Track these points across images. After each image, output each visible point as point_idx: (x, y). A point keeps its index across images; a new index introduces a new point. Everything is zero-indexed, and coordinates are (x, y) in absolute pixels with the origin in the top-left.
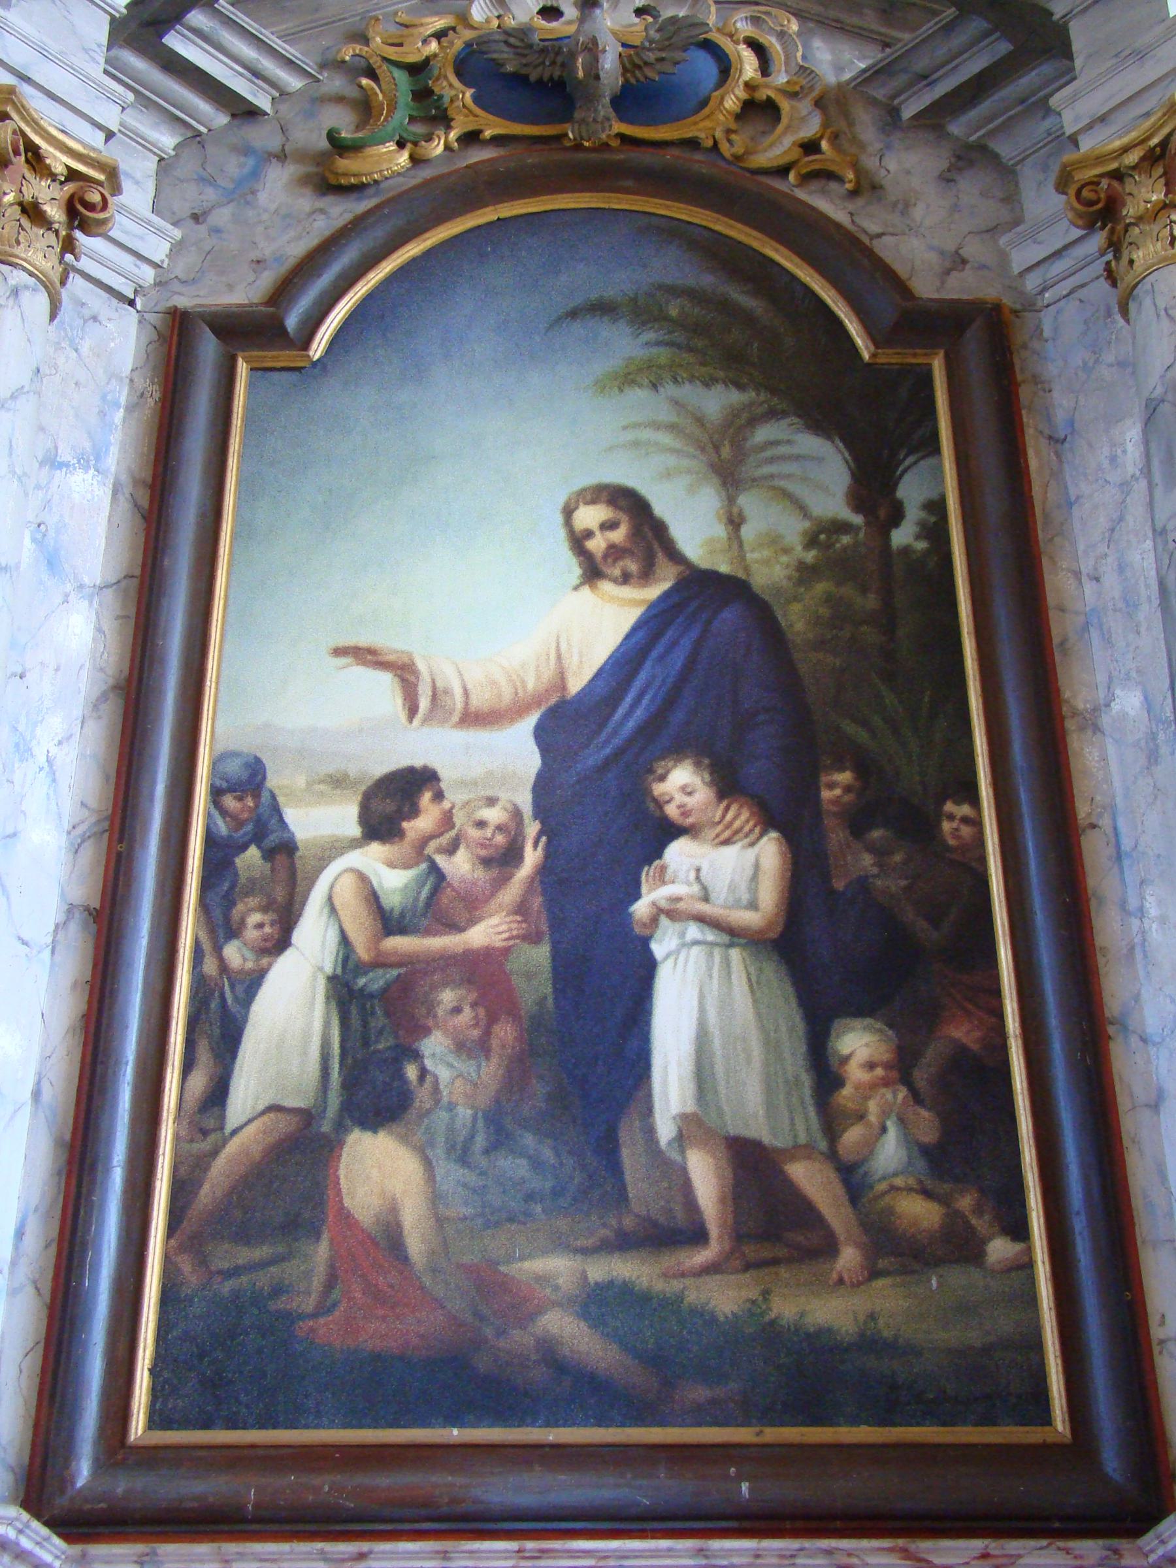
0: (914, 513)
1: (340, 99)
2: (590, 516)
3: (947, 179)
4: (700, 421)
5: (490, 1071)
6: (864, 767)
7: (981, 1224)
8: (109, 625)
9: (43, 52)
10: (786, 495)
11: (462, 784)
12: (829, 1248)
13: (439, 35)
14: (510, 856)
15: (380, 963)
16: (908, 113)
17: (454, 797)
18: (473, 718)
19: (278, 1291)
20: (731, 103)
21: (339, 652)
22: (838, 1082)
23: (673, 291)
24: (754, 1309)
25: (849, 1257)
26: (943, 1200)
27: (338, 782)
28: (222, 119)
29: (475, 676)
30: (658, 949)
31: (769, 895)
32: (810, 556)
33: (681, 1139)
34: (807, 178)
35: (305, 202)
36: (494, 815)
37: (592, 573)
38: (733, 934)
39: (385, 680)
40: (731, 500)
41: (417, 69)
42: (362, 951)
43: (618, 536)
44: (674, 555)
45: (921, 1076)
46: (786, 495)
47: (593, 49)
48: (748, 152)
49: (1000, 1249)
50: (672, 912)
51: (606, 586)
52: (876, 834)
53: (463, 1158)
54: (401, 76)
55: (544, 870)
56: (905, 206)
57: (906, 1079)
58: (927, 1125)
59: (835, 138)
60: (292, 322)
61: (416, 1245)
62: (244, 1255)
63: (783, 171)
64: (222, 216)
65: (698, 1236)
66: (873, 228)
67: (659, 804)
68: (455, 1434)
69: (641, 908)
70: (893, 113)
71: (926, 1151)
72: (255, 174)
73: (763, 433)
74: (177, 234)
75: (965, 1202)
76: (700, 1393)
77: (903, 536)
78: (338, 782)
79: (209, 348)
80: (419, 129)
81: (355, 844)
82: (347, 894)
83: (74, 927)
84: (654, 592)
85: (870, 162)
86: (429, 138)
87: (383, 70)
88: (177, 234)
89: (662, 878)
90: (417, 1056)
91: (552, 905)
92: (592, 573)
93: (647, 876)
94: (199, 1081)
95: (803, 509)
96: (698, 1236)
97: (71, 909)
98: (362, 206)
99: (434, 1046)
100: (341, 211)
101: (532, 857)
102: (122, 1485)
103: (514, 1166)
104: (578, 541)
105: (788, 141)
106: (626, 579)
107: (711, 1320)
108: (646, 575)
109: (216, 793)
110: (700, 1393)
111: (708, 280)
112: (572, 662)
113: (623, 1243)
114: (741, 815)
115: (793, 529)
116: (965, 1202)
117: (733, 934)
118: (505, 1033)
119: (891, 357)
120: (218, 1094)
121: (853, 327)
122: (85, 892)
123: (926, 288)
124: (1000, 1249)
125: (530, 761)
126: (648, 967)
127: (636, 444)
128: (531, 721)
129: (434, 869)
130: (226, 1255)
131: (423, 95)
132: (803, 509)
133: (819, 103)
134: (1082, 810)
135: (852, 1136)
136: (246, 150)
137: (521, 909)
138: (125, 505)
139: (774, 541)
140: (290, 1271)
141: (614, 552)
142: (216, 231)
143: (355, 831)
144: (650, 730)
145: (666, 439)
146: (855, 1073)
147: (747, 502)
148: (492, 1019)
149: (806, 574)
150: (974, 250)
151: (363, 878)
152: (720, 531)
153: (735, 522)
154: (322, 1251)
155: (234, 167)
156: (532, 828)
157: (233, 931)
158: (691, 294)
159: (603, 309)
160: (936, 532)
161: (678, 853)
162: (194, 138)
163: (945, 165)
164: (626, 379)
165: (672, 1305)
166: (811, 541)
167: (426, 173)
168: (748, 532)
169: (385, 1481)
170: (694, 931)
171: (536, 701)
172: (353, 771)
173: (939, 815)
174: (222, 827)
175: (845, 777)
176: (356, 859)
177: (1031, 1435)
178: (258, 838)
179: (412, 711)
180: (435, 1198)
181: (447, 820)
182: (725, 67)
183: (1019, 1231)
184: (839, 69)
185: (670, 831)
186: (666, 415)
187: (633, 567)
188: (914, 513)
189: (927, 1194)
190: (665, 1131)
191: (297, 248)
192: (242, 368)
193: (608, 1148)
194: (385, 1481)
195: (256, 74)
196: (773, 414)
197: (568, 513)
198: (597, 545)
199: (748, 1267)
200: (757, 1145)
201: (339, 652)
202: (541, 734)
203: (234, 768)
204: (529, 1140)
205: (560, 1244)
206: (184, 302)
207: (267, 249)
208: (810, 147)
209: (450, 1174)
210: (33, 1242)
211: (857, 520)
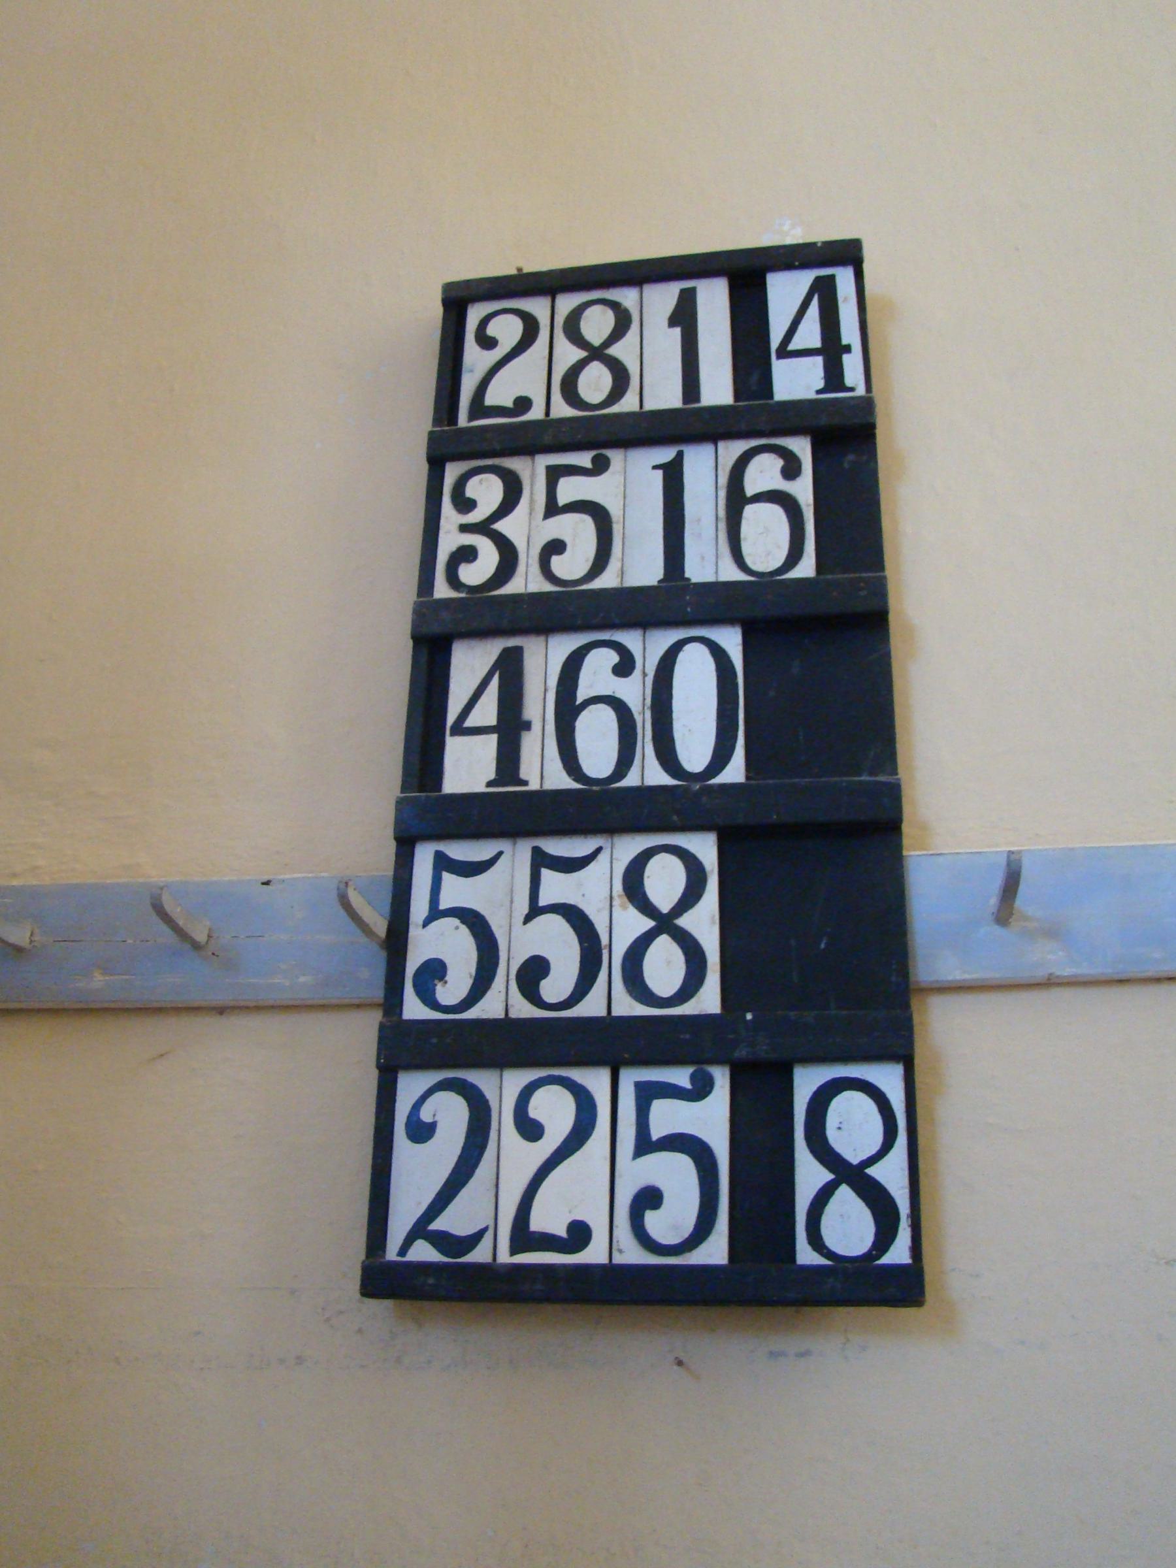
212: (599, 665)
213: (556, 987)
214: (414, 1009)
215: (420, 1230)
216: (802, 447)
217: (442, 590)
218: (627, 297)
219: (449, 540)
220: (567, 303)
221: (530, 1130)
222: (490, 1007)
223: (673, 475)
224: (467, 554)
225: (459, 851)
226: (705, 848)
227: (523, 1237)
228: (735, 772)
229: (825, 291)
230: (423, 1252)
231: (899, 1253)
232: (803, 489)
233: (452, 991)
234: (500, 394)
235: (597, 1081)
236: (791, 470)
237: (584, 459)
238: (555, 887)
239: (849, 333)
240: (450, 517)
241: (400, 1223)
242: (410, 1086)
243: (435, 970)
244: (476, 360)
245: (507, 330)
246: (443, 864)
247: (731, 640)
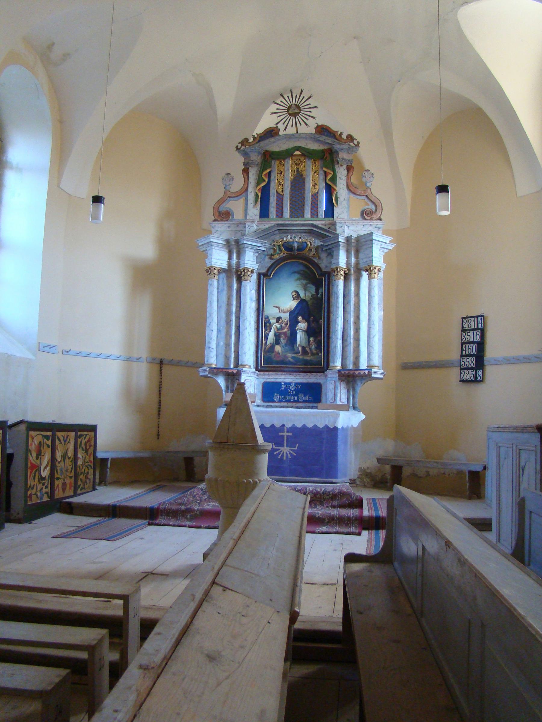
0: (320, 293)
1: (272, 248)
2: (294, 294)
3: (327, 257)
4: (303, 284)
5: (285, 341)
6: (314, 317)
7: (319, 352)
8: (256, 304)
9: (248, 261)
10: (310, 292)
11: (284, 318)
12: (308, 354)
13: (281, 242)
14: (287, 324)
15: (277, 333)
16: (324, 249)
17: (283, 319)
18: (284, 312)
19: (272, 356)
20: (308, 249)
21: (274, 306)
22: (310, 342)
23: (302, 270)
24: (303, 358)
25: (309, 355)
26: (316, 350)
27: (274, 318)
28: (262, 251)
29: (284, 308)
30: (298, 332)
31: (306, 328)
32: (311, 297)
33: (299, 346)
34: (314, 257)
35: (269, 260)
36: (286, 321)
37: (294, 299)
38: (303, 331)
39: (277, 309)
40: (305, 292)
41: (279, 246)
42: (276, 332)
43: (296, 295)
44: (301, 297)
45: (316, 342)
46: (310, 292)
47: (294, 247)
48: (309, 254)
49: (320, 354)
50: (299, 329)
51: (295, 300)
52: (314, 323)
53: (283, 347)
54: (278, 247)
55: (289, 325)
56: (323, 260)
57: (315, 342)
58: (316, 345)
59: (317, 254)
60: (269, 274)
61: (280, 353)
62: (269, 354)
63: (312, 257)
64: (262, 262)
65: (300, 353)
66: (319, 263)
67: (298, 320)
68: (283, 366)
69: (296, 328)
70: (323, 249)
71: (316, 347)
72: (265, 257)
73: (308, 285)
74: (258, 265)
75: (318, 351)
76: (299, 363)
77: (319, 296)
78: (274, 318)
79: (262, 276)
80: (279, 252)
81: (276, 323)
82: (275, 327)
83: (255, 330)
84: (299, 301)
85: (320, 255)
86: (280, 254)
87: (276, 246)
88: (258, 265)
89: (298, 326)
90: (280, 340)
91: (290, 329)
92: (294, 299)
93: (297, 326)
94: (265, 341)
95: (311, 293)
96: (300, 353)
97: (255, 328)
98: (275, 261)
99: (281, 339)
100: (273, 261)
101: (289, 324)
102: (263, 369)
103: (287, 348)
104: (293, 296)
105: (313, 254)
106: (296, 300)
107: (299, 358)
108: (298, 299)
109: (265, 319)
110: (299, 363)
111: (304, 269)
112: (292, 307)
113: (295, 353)
114: (304, 321)
115: (310, 295)
116: (318, 351)
117: (303, 331)
118: (286, 338)
119: (319, 277)
120: (266, 343)
121: (317, 274)
122: (256, 327)
123: (324, 270)
124: (320, 354)
125: (289, 316)
126: (297, 333)
127: (297, 286)
128: (289, 313)
129: (281, 326)
130: (268, 354)
131: (279, 248)
132: (311, 293)
133: (315, 249)
134: (330, 321)
135: (311, 346)
136: (264, 254)
137: (288, 328)
138: (256, 292)
139: (308, 296)
140: (272, 355)
141: (295, 297)
142: (262, 264)
143: (275, 322)
144: (298, 313)
145: (300, 286)
146: (311, 341)
147: (307, 292)
148: (286, 337)
149: (311, 299)
150: (328, 265)
151: (276, 326)
152: (304, 295)
153: (305, 294)
154: (274, 354)
155: (263, 256)
156: (289, 322)
157: (267, 330)
158: (304, 271)
159: (295, 272)
160: (322, 295)
161: (299, 324)
162: (259, 254)
163: (326, 256)
164: (297, 280)
165: (297, 357)
166: (311, 296)
167: (280, 257)
168: (306, 295)
169: (279, 369)
170: (300, 330)
171: (289, 311)
172: (275, 317)
173: (319, 321)
174: (266, 322)
175: (312, 318)
176: (275, 324)
177: (321, 366)
178: (268, 323)
179: (280, 312)
180: (281, 350)
181: (282, 321)
182: (307, 245)
183: (322, 353)
184: (318, 244)
185: (299, 322)
186: (300, 283)
187: (297, 298)
188: (320, 293)
189: (315, 350)
190: (298, 345)
191: (269, 265)
192: (265, 279)
193: (294, 347)
194: (279, 369)
195: (264, 247)
196: (309, 283)
197: (292, 293)
198: (294, 296)
199: (303, 355)
200: (303, 347)
201: (274, 306)
202: (289, 314)
203: (266, 317)
204: (288, 346)
205: (290, 353)
206: (259, 271)
207: (266, 266)
208: (314, 254)
209: (283, 348)
210: (255, 353)
211: (315, 294)
212: (470, 346)
213: (468, 366)
214: (462, 367)
215: (462, 379)
216: (480, 331)
217: (462, 341)
218: (471, 319)
219: (463, 338)
220: (468, 319)
221: (466, 373)
222: (465, 367)
223: (473, 332)
224: (463, 339)
225: (463, 358)
226: (474, 357)
227: (466, 379)
228: (476, 353)
229: (481, 319)
230: (462, 380)
231: (481, 379)
232: (480, 334)
233: (463, 366)
234: (465, 327)
235: (469, 370)
236: (479, 333)
237: (469, 332)
238: (468, 360)
239: (483, 322)
240: (463, 336)
241: (461, 378)
242: (461, 371)
243: (462, 365)
244: (464, 324)
245: (465, 321)
246: (463, 359)
247: (476, 344)
